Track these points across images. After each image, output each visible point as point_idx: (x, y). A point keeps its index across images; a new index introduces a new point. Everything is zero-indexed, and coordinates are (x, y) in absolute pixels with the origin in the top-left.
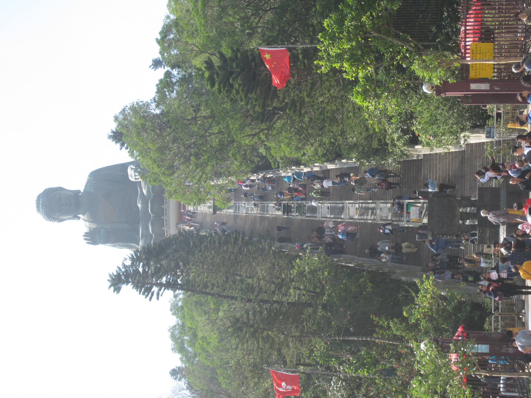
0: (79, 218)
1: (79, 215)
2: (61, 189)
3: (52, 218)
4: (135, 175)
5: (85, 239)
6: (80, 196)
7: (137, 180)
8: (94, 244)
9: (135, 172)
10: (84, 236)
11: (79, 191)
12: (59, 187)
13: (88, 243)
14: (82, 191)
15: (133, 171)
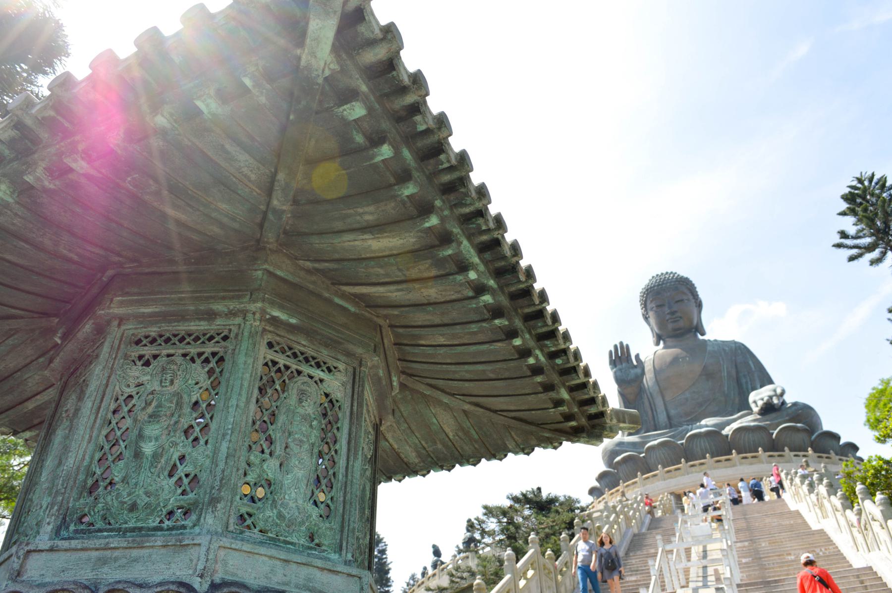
0: (658, 344)
1: (662, 342)
2: (700, 305)
3: (646, 301)
4: (762, 399)
5: (616, 347)
6: (696, 336)
7: (753, 406)
8: (610, 364)
9: (771, 397)
10: (621, 343)
11: (703, 334)
12: (701, 302)
13: (611, 352)
14: (705, 337)
15: (772, 393)
